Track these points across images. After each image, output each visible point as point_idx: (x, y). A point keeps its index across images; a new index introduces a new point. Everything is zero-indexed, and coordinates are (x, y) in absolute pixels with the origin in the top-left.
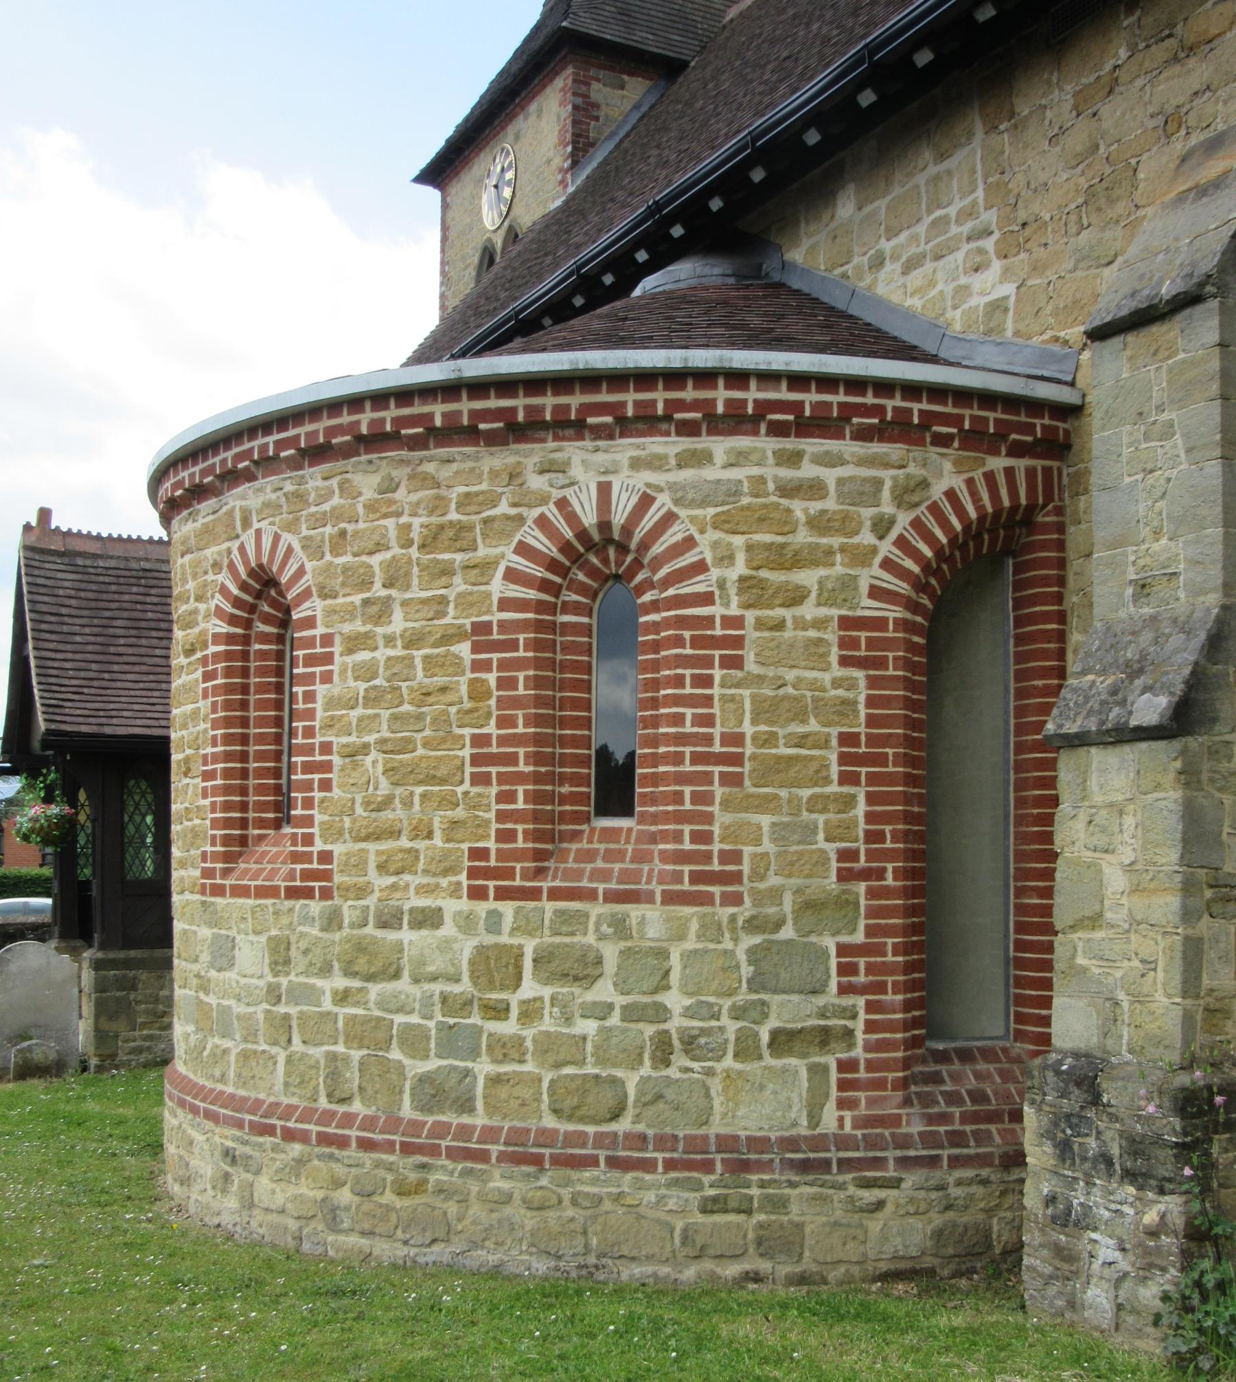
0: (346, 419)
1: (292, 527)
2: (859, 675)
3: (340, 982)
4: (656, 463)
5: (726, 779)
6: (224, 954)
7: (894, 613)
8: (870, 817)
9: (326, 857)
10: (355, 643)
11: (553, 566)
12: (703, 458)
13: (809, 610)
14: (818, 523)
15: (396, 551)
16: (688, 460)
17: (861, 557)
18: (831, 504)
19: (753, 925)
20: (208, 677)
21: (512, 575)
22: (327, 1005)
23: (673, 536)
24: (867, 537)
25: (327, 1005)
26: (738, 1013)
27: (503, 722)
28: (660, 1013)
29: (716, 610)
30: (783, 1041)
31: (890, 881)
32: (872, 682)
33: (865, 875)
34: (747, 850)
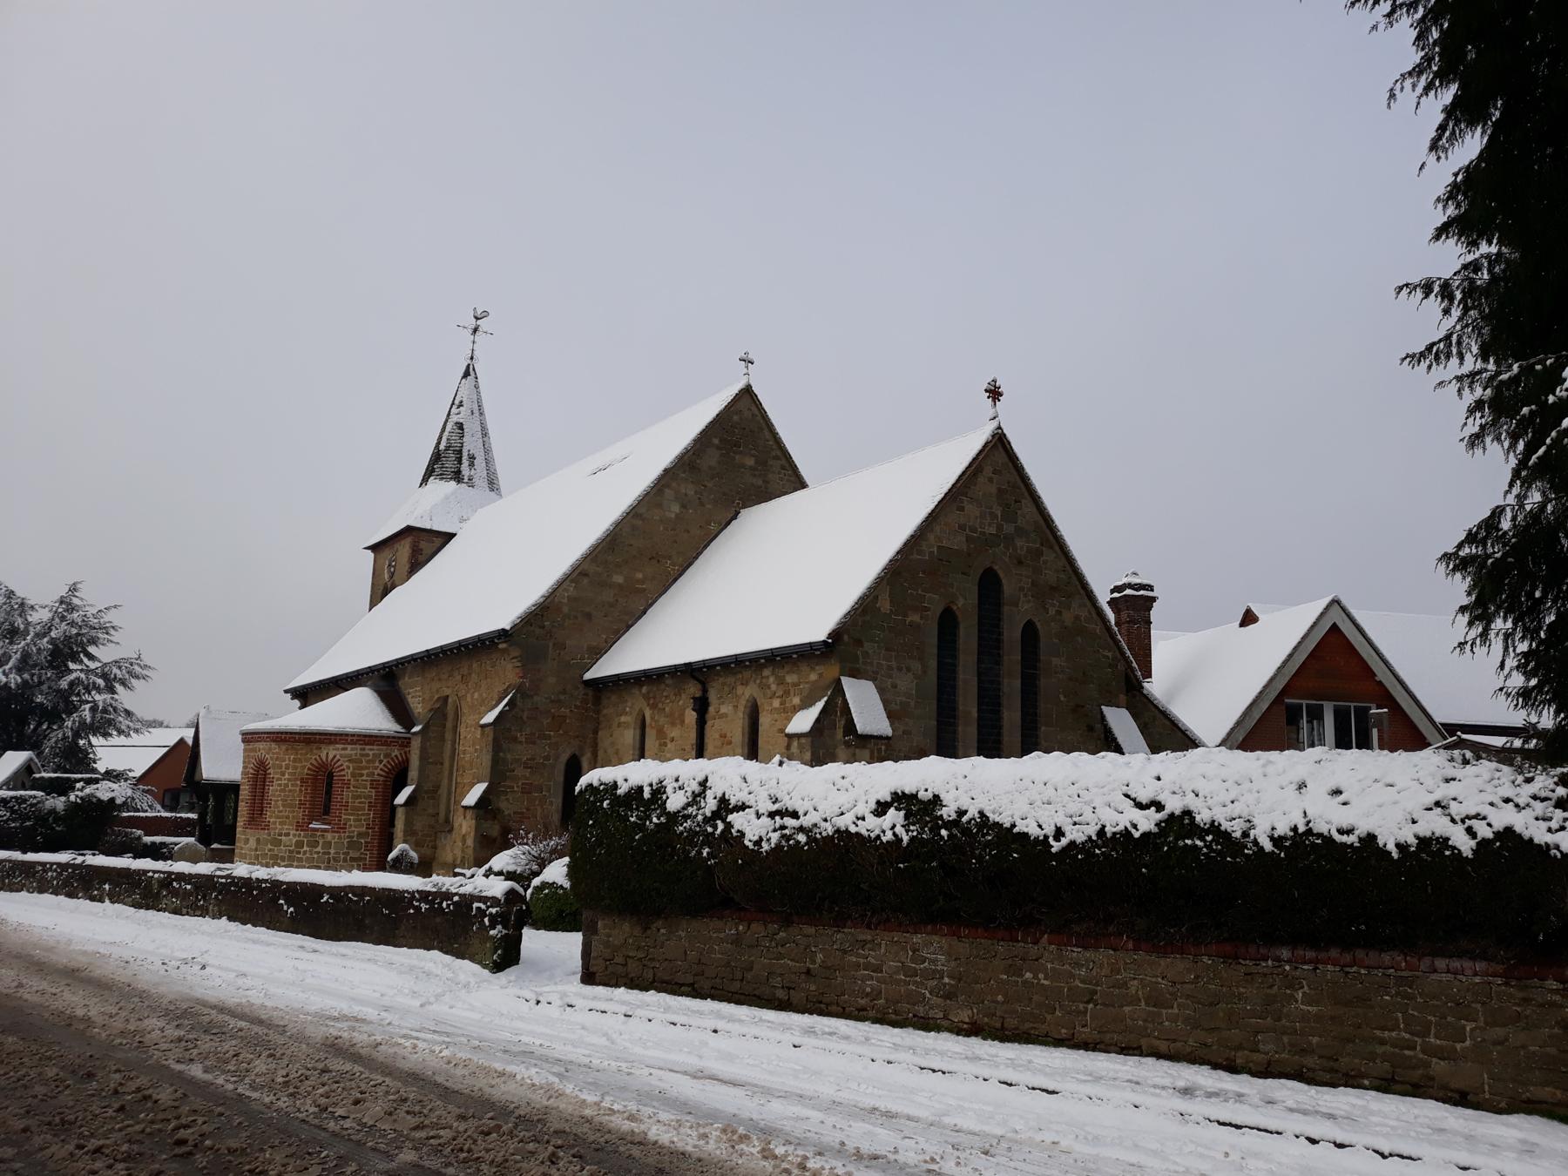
0: (280, 735)
1: (268, 754)
2: (373, 790)
4: (338, 749)
5: (346, 810)
6: (247, 841)
7: (382, 779)
8: (373, 817)
9: (269, 822)
10: (278, 779)
11: (317, 767)
12: (346, 749)
14: (368, 762)
15: (287, 762)
16: (343, 749)
17: (376, 768)
18: (371, 758)
19: (348, 837)
20: (249, 781)
21: (309, 769)
22: (267, 852)
23: (339, 763)
24: (377, 764)
25: (267, 852)
26: (343, 854)
27: (305, 797)
28: (329, 853)
29: (346, 778)
30: (353, 859)
31: (376, 829)
32: (376, 792)
33: (371, 828)
34: (348, 823)
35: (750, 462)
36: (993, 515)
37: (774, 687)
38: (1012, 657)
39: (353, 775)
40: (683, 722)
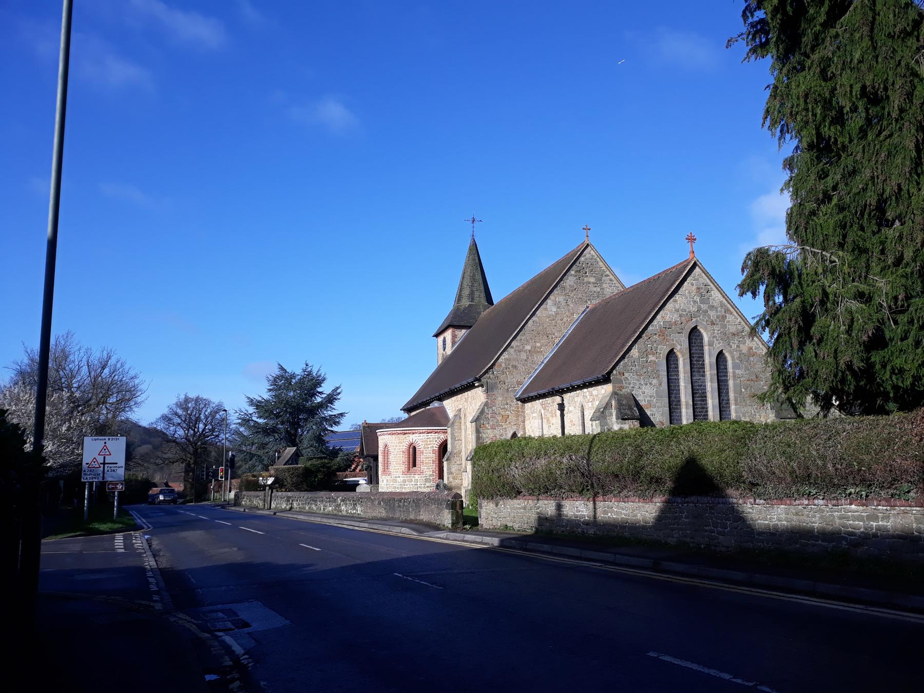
3: (392, 483)
13: (429, 449)
14: (430, 441)
17: (434, 444)
19: (425, 477)
24: (434, 442)
35: (592, 280)
36: (695, 302)
37: (588, 397)
38: (710, 372)
39: (425, 448)
40: (556, 415)
